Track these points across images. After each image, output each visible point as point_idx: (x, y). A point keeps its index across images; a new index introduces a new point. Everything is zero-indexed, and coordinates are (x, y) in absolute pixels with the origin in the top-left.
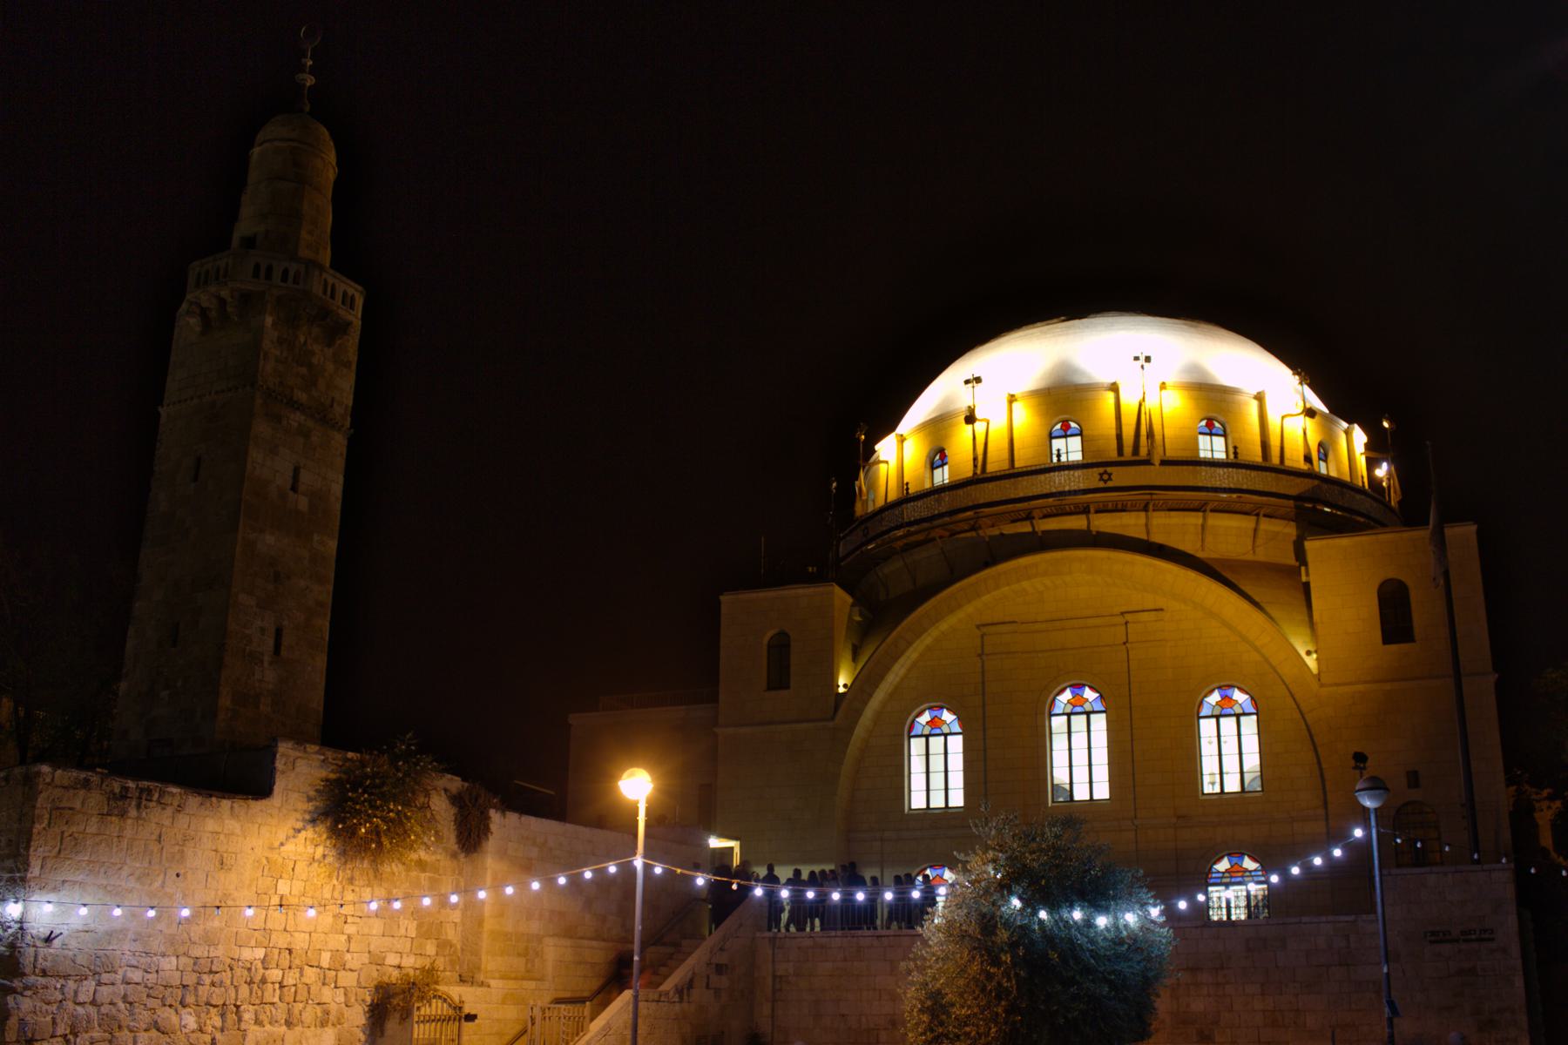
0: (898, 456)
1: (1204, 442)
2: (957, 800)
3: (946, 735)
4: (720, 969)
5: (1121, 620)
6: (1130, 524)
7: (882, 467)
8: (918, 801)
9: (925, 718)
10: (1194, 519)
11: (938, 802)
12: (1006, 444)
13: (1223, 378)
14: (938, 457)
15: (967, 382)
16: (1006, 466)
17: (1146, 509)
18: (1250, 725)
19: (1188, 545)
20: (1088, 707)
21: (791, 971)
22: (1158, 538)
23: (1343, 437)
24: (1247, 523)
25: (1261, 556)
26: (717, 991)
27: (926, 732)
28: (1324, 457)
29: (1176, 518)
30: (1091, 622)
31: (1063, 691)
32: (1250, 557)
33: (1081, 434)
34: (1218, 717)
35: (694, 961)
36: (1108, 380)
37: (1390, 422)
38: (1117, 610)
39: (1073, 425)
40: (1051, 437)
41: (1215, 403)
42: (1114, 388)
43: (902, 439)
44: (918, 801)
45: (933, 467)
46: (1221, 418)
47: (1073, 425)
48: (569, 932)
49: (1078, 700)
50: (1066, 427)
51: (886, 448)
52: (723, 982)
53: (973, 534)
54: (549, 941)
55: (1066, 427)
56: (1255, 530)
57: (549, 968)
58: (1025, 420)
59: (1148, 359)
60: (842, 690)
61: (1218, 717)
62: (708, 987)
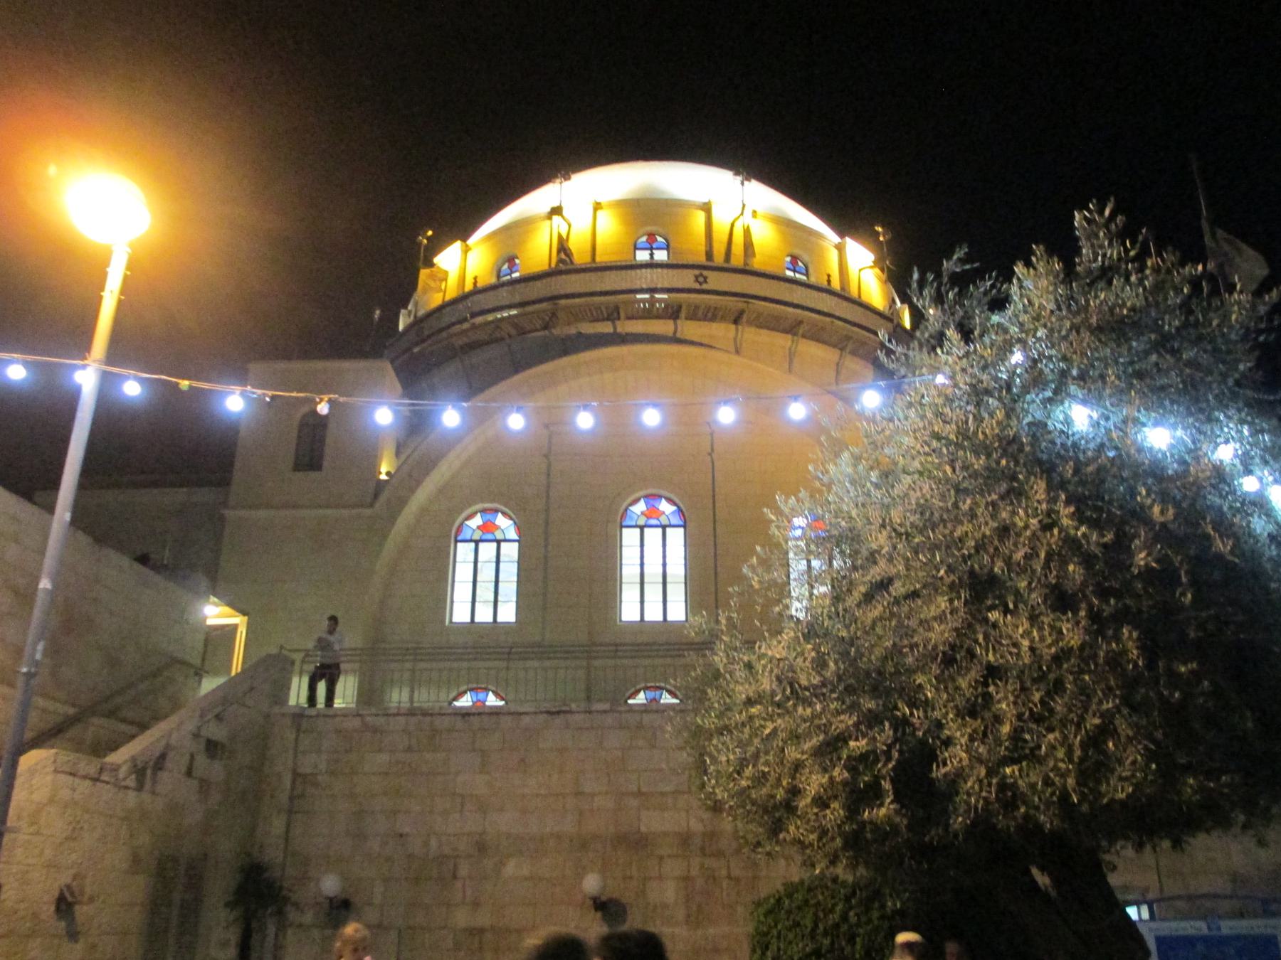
2: (508, 614)
3: (499, 542)
4: (212, 747)
8: (460, 614)
9: (477, 521)
11: (484, 615)
12: (588, 247)
20: (664, 520)
21: (323, 767)
26: (204, 786)
27: (476, 537)
31: (636, 501)
36: (701, 198)
39: (659, 239)
40: (636, 248)
42: (707, 208)
44: (460, 614)
46: (806, 258)
47: (659, 239)
49: (652, 512)
50: (652, 237)
52: (215, 770)
53: (547, 332)
55: (652, 237)
60: (383, 477)
62: (189, 773)
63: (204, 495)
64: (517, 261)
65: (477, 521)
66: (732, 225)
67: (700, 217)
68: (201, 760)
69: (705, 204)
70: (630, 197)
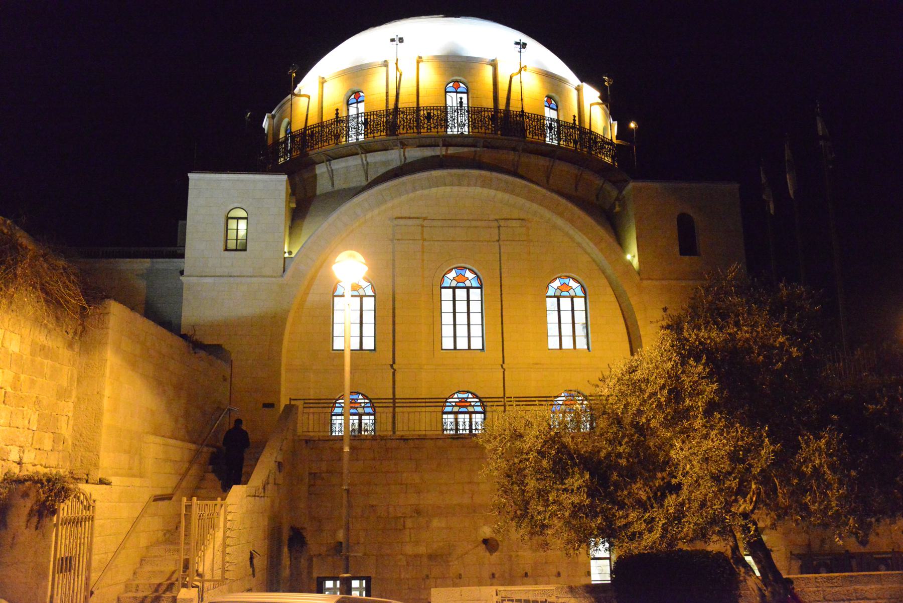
1: (547, 109)
5: (495, 224)
14: (355, 96)
15: (393, 40)
20: (468, 284)
24: (572, 170)
33: (467, 93)
36: (489, 57)
38: (492, 217)
39: (462, 85)
42: (494, 64)
43: (323, 81)
45: (348, 104)
46: (557, 98)
48: (156, 432)
49: (461, 278)
51: (308, 85)
54: (152, 438)
57: (149, 464)
64: (361, 94)
66: (511, 78)
67: (488, 71)
69: (493, 60)
70: (439, 54)
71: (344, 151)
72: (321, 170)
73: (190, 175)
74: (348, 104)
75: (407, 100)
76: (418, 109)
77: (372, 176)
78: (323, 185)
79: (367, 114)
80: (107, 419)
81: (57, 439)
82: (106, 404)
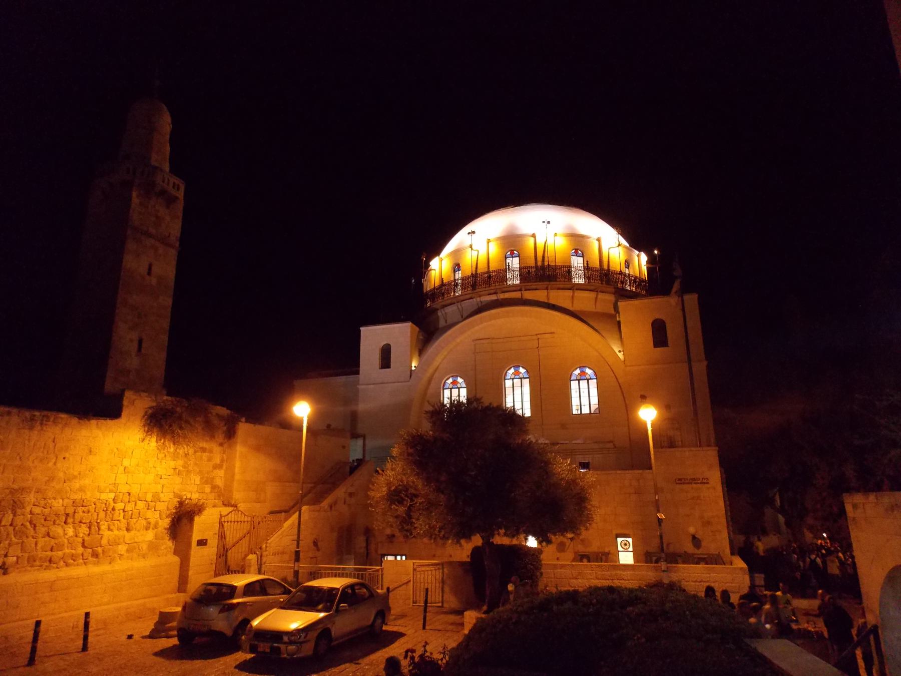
0: (439, 267)
5: (535, 337)
6: (540, 295)
7: (433, 272)
9: (450, 380)
10: (569, 293)
12: (486, 261)
13: (582, 231)
14: (457, 267)
16: (486, 270)
17: (547, 289)
18: (593, 383)
19: (567, 305)
22: (552, 302)
23: (636, 258)
24: (592, 295)
25: (600, 309)
28: (627, 266)
29: (561, 293)
30: (523, 338)
32: (594, 310)
34: (579, 380)
35: (340, 492)
37: (658, 250)
41: (578, 243)
42: (534, 236)
45: (455, 272)
49: (517, 373)
50: (512, 253)
51: (434, 263)
55: (512, 253)
56: (596, 298)
58: (495, 251)
59: (549, 222)
61: (579, 380)
63: (352, 378)
65: (450, 380)
67: (532, 240)
68: (348, 498)
71: (449, 302)
72: (439, 314)
73: (364, 330)
74: (455, 272)
75: (482, 268)
76: (488, 272)
77: (465, 315)
78: (442, 323)
79: (463, 279)
80: (237, 477)
81: (214, 487)
82: (237, 470)
